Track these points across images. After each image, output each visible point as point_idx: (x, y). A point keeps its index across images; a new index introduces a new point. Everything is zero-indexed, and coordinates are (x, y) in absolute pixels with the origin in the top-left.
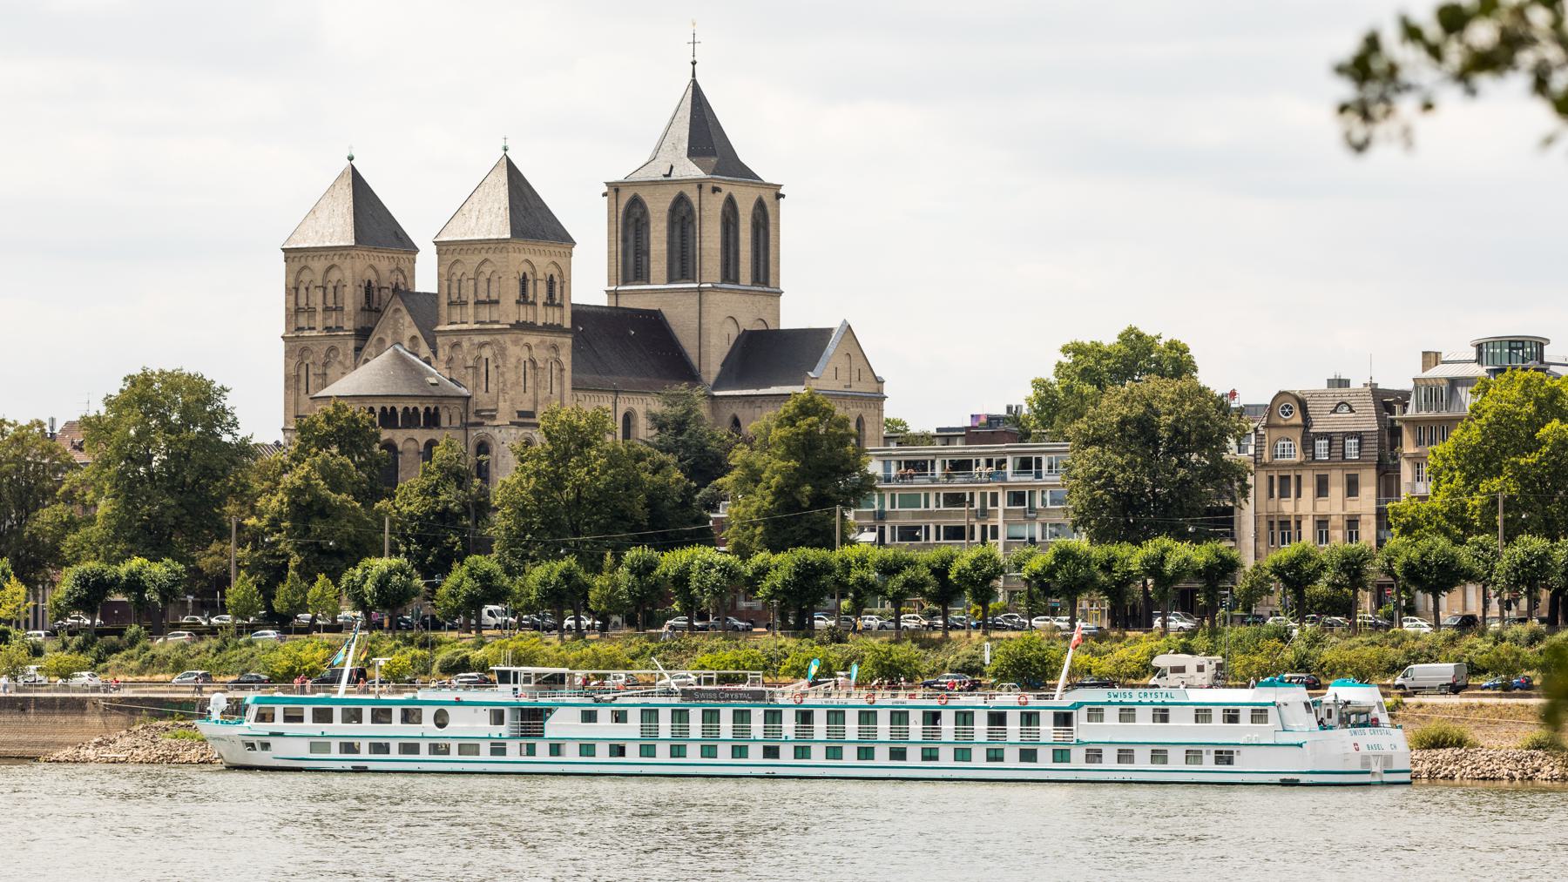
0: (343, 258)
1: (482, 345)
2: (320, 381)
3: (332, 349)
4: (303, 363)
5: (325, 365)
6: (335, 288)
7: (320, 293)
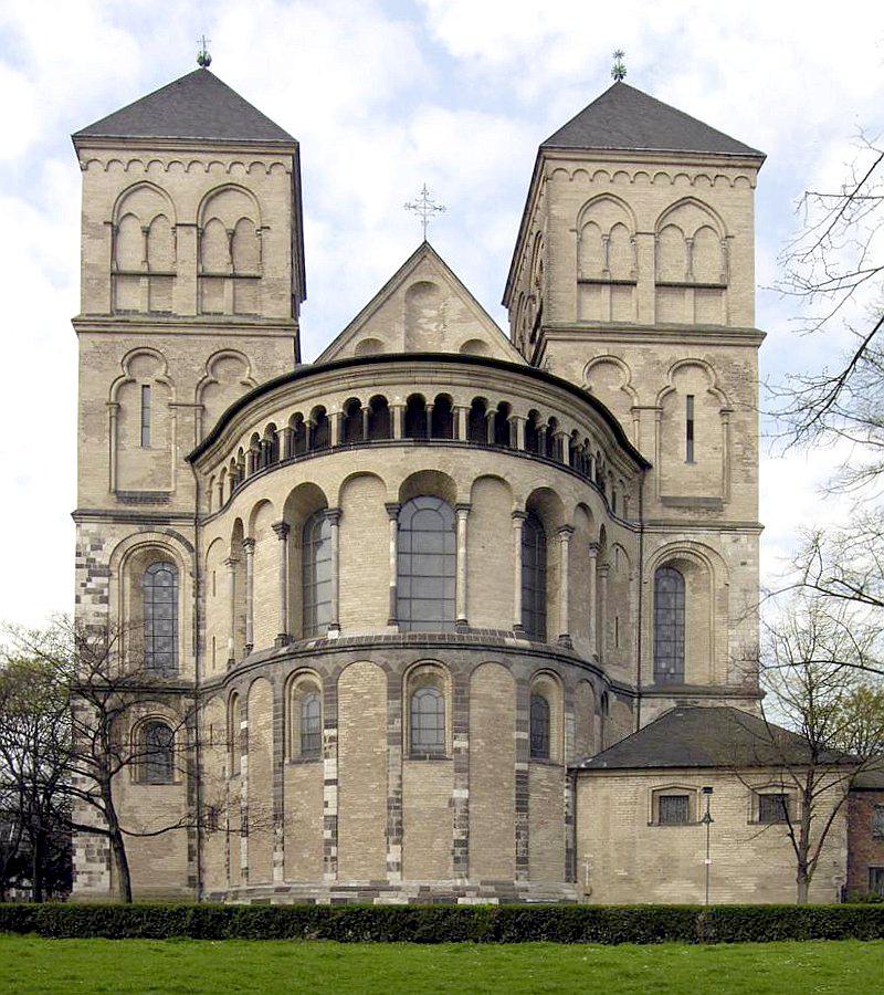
0: (260, 170)
1: (680, 367)
2: (190, 419)
3: (224, 356)
4: (134, 381)
6: (232, 235)
7: (188, 240)
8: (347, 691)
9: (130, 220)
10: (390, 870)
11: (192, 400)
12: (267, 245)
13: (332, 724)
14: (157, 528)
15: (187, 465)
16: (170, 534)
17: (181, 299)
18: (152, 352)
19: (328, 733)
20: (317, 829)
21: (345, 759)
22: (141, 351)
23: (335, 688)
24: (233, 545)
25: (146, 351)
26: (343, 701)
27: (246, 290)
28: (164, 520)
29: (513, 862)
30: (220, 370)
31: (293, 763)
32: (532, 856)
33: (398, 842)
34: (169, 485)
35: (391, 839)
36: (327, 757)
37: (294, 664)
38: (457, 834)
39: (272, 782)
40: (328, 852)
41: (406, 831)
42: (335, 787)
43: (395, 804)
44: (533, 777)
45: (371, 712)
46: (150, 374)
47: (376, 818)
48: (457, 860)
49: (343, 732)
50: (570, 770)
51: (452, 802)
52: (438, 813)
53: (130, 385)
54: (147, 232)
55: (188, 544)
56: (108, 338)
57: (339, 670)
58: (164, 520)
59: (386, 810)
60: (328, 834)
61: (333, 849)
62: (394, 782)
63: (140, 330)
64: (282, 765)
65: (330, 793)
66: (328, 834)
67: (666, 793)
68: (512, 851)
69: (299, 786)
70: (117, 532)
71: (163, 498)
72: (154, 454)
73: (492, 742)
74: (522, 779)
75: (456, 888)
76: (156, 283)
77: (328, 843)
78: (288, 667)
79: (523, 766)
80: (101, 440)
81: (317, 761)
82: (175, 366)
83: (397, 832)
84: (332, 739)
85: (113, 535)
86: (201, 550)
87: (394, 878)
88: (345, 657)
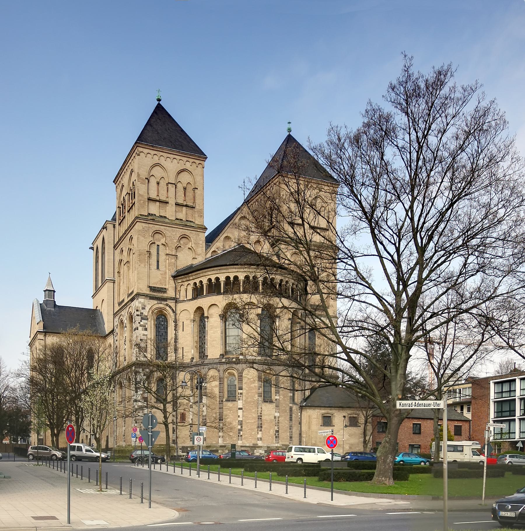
2: (173, 261)
3: (184, 237)
4: (154, 243)
5: (177, 248)
6: (185, 189)
7: (172, 188)
8: (246, 377)
9: (152, 177)
10: (258, 440)
11: (174, 254)
12: (197, 195)
13: (241, 388)
14: (163, 302)
15: (172, 278)
16: (167, 305)
17: (170, 212)
18: (161, 232)
19: (240, 391)
20: (235, 425)
21: (245, 401)
22: (157, 231)
23: (242, 376)
24: (194, 315)
25: (159, 232)
26: (245, 380)
27: (190, 211)
28: (165, 299)
29: (289, 438)
30: (182, 242)
31: (227, 400)
32: (293, 436)
33: (261, 431)
34: (165, 285)
35: (259, 429)
36: (239, 400)
37: (228, 366)
38: (276, 428)
39: (218, 407)
40: (239, 433)
41: (263, 427)
42: (242, 410)
43: (260, 418)
44: (293, 409)
45: (253, 385)
46: (159, 241)
47: (254, 422)
48: (276, 437)
49: (243, 391)
50: (300, 406)
51: (275, 417)
52: (271, 421)
53: (153, 244)
54: (158, 183)
55: (173, 310)
56: (147, 225)
57: (243, 370)
58: (165, 299)
59: (257, 419)
60: (239, 427)
61: (241, 432)
62: (260, 409)
63: (157, 223)
64: (222, 401)
65: (240, 412)
66: (239, 427)
67: (325, 415)
68: (288, 434)
69: (229, 409)
70: (150, 303)
71: (163, 290)
72: (161, 272)
73: (284, 397)
74: (291, 409)
75: (276, 447)
76: (161, 204)
77: (240, 430)
78: (225, 366)
79: (291, 405)
80: (145, 265)
81: (235, 401)
82: (168, 239)
83: (260, 427)
84: (241, 394)
85: (149, 304)
86: (177, 312)
87: (260, 443)
88: (244, 366)
